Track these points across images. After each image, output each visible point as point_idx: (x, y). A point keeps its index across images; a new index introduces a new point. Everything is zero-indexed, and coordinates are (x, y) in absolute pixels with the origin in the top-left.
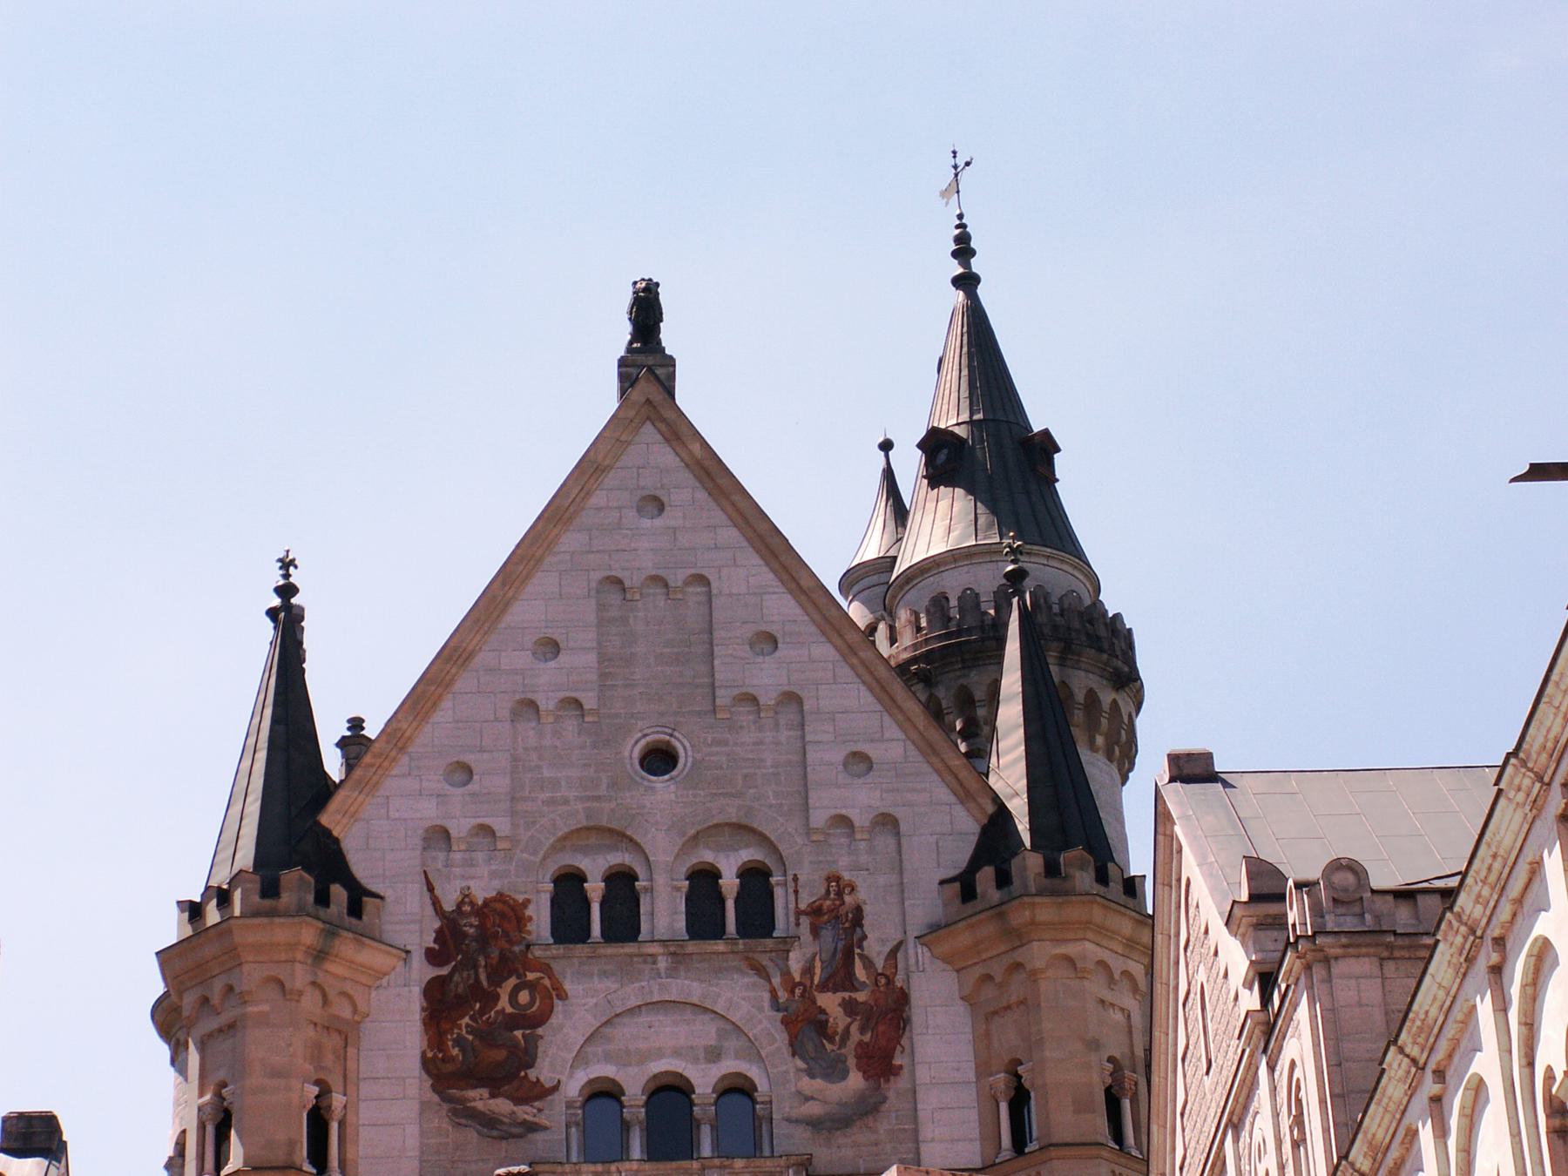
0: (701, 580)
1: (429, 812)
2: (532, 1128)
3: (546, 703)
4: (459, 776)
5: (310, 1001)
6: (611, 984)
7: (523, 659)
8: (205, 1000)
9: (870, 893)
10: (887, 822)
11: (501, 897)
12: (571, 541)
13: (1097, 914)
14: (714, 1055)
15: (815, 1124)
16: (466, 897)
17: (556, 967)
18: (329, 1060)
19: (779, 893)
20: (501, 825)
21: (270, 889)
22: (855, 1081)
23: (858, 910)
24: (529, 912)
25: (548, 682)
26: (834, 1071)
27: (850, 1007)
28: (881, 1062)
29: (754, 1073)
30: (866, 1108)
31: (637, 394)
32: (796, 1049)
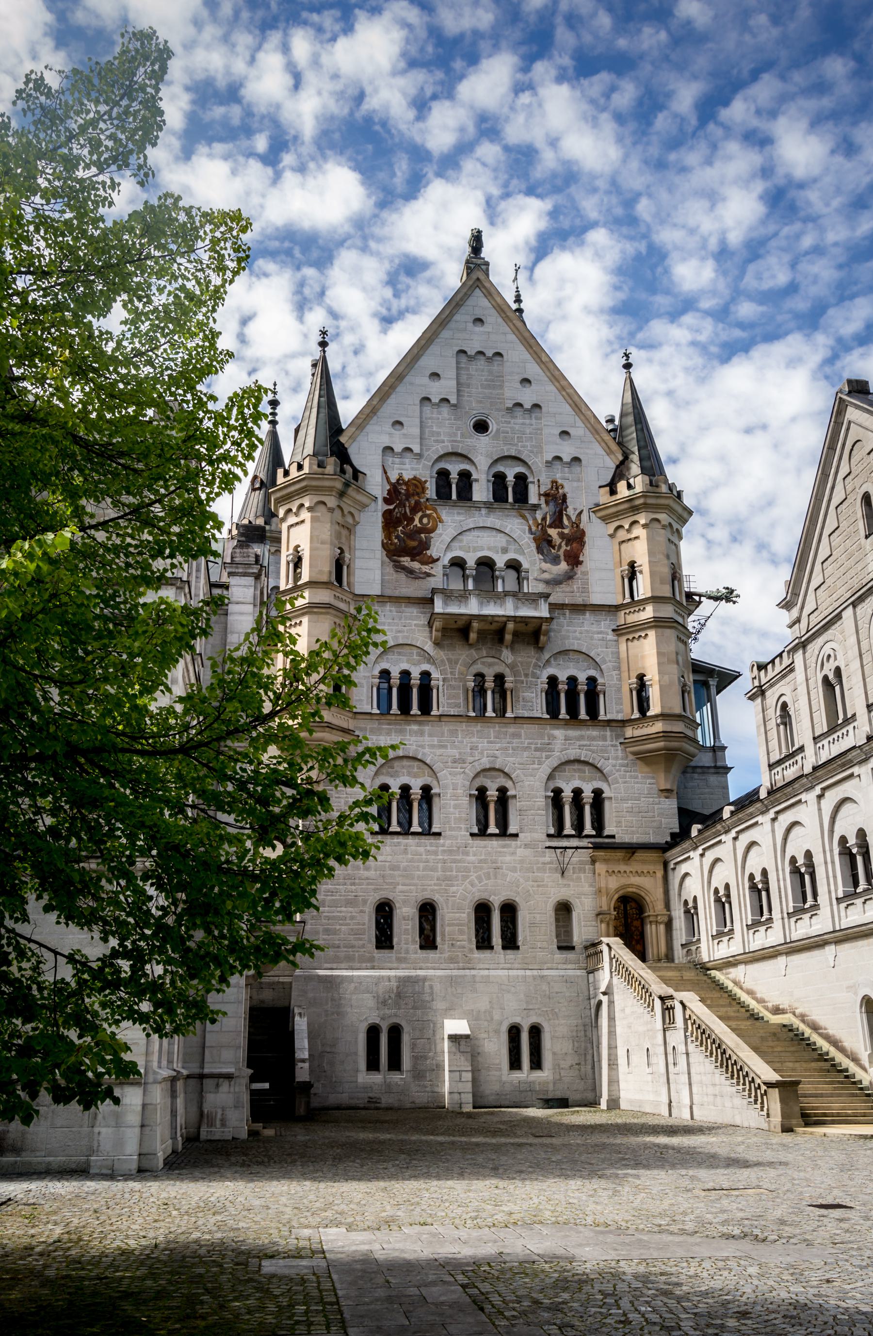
0: (499, 354)
1: (386, 441)
2: (429, 575)
3: (435, 399)
4: (398, 427)
5: (338, 513)
6: (461, 518)
7: (426, 380)
8: (290, 510)
9: (567, 488)
10: (576, 460)
11: (415, 478)
12: (445, 334)
13: (670, 502)
14: (505, 550)
15: (547, 582)
16: (400, 478)
17: (439, 508)
18: (344, 540)
19: (531, 486)
20: (416, 449)
21: (321, 465)
22: (563, 566)
23: (564, 496)
24: (428, 485)
25: (436, 391)
26: (555, 561)
27: (562, 536)
28: (574, 560)
29: (520, 558)
30: (569, 577)
31: (474, 276)
32: (539, 550)
